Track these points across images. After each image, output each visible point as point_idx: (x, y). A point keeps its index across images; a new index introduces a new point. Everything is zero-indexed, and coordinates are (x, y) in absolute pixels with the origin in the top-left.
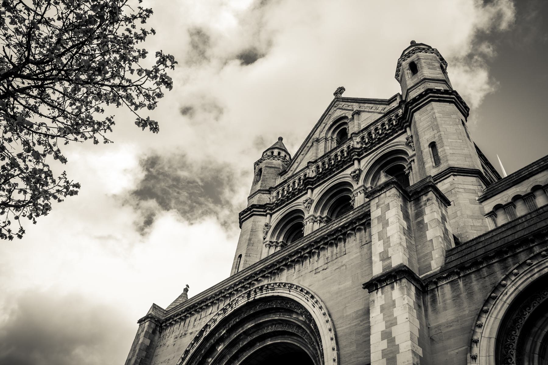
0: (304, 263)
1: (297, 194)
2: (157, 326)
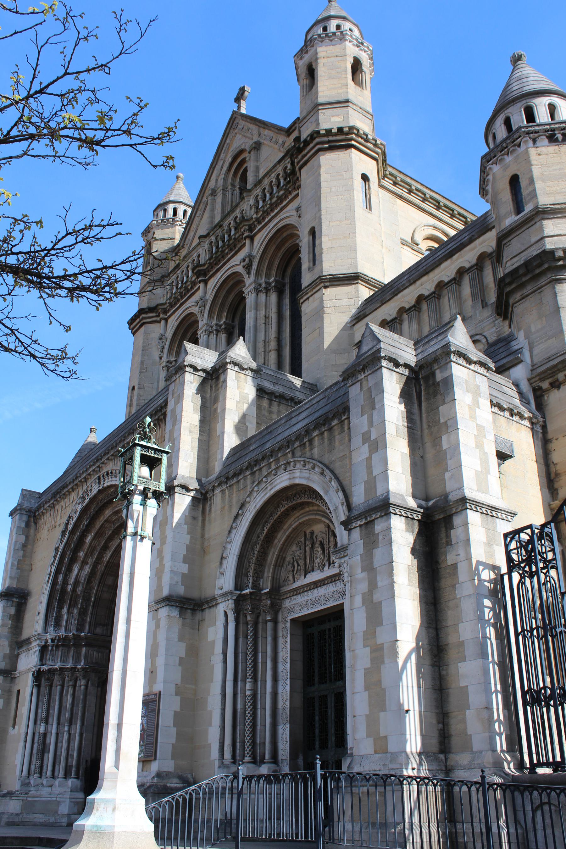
2: (29, 516)
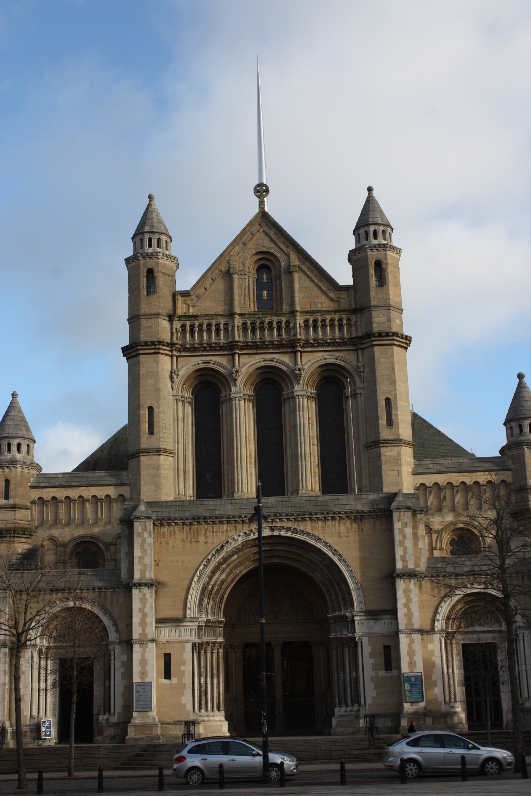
1: (217, 350)
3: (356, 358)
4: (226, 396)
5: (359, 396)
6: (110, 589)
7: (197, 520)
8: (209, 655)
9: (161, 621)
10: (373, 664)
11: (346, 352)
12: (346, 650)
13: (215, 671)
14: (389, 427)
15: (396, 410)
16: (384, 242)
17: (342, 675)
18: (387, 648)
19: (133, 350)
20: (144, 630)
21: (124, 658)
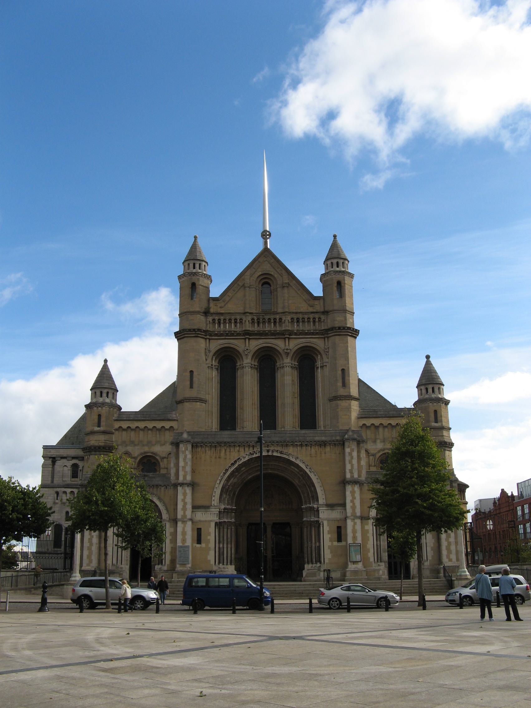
0: (303, 448)
1: (235, 336)
3: (324, 343)
4: (240, 365)
5: (325, 367)
6: (163, 486)
7: (220, 444)
8: (225, 530)
9: (195, 508)
10: (329, 538)
11: (317, 339)
12: (313, 529)
13: (229, 540)
14: (344, 387)
15: (349, 376)
16: (343, 270)
17: (310, 544)
18: (339, 528)
19: (181, 334)
20: (184, 513)
21: (172, 530)
